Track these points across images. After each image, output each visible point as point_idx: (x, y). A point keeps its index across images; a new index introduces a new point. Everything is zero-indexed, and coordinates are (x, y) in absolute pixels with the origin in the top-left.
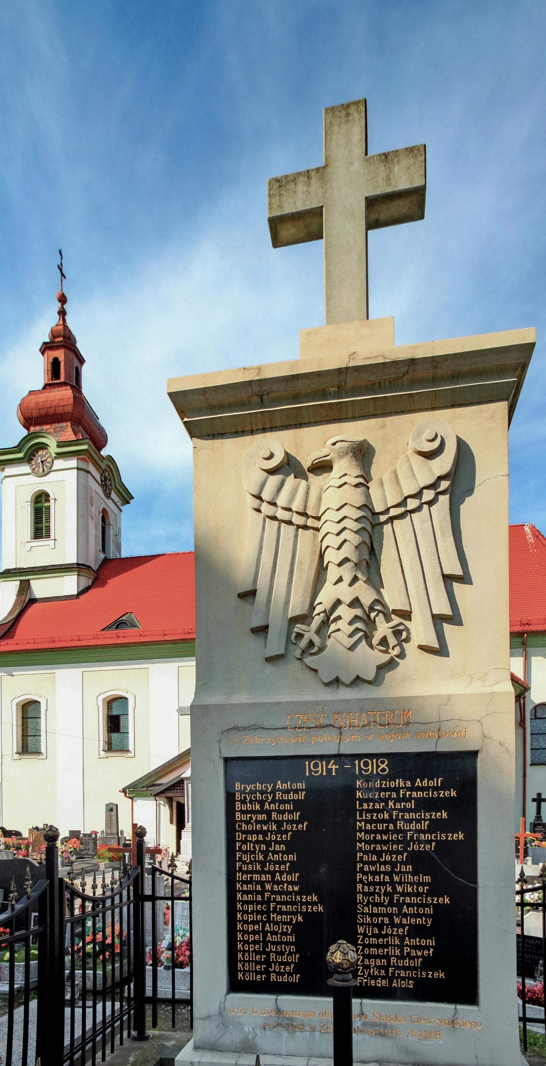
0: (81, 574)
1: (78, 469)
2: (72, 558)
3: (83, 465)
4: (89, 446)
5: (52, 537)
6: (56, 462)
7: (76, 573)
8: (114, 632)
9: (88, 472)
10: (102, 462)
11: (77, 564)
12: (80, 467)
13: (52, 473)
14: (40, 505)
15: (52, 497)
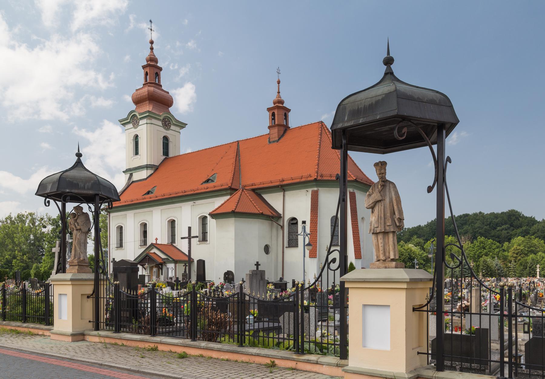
0: (148, 169)
1: (147, 123)
2: (144, 163)
3: (149, 121)
4: (148, 113)
5: (139, 154)
6: (140, 121)
7: (146, 169)
8: (146, 196)
9: (152, 124)
10: (160, 117)
11: (147, 165)
12: (148, 122)
13: (139, 127)
14: (137, 140)
15: (139, 137)
